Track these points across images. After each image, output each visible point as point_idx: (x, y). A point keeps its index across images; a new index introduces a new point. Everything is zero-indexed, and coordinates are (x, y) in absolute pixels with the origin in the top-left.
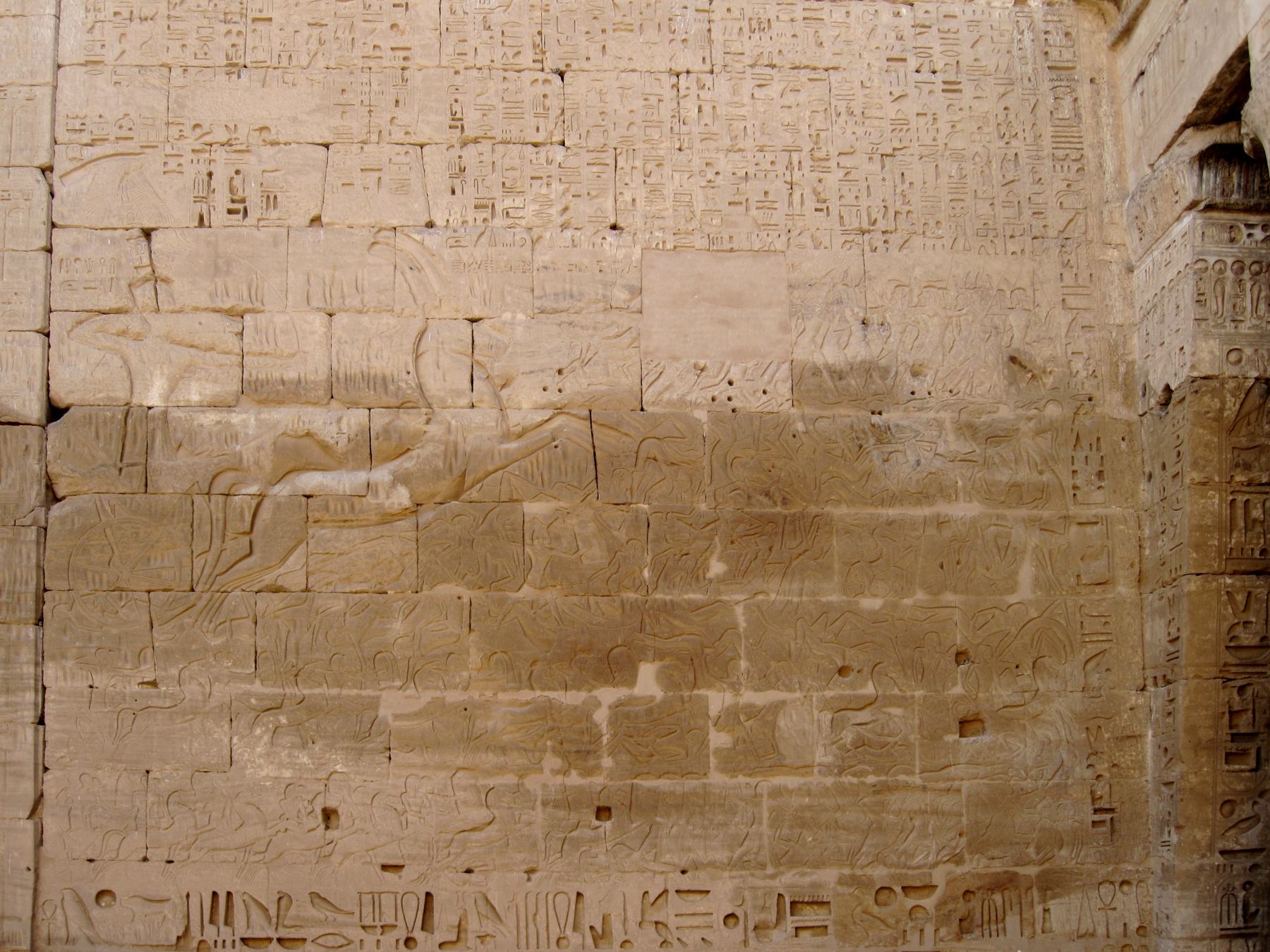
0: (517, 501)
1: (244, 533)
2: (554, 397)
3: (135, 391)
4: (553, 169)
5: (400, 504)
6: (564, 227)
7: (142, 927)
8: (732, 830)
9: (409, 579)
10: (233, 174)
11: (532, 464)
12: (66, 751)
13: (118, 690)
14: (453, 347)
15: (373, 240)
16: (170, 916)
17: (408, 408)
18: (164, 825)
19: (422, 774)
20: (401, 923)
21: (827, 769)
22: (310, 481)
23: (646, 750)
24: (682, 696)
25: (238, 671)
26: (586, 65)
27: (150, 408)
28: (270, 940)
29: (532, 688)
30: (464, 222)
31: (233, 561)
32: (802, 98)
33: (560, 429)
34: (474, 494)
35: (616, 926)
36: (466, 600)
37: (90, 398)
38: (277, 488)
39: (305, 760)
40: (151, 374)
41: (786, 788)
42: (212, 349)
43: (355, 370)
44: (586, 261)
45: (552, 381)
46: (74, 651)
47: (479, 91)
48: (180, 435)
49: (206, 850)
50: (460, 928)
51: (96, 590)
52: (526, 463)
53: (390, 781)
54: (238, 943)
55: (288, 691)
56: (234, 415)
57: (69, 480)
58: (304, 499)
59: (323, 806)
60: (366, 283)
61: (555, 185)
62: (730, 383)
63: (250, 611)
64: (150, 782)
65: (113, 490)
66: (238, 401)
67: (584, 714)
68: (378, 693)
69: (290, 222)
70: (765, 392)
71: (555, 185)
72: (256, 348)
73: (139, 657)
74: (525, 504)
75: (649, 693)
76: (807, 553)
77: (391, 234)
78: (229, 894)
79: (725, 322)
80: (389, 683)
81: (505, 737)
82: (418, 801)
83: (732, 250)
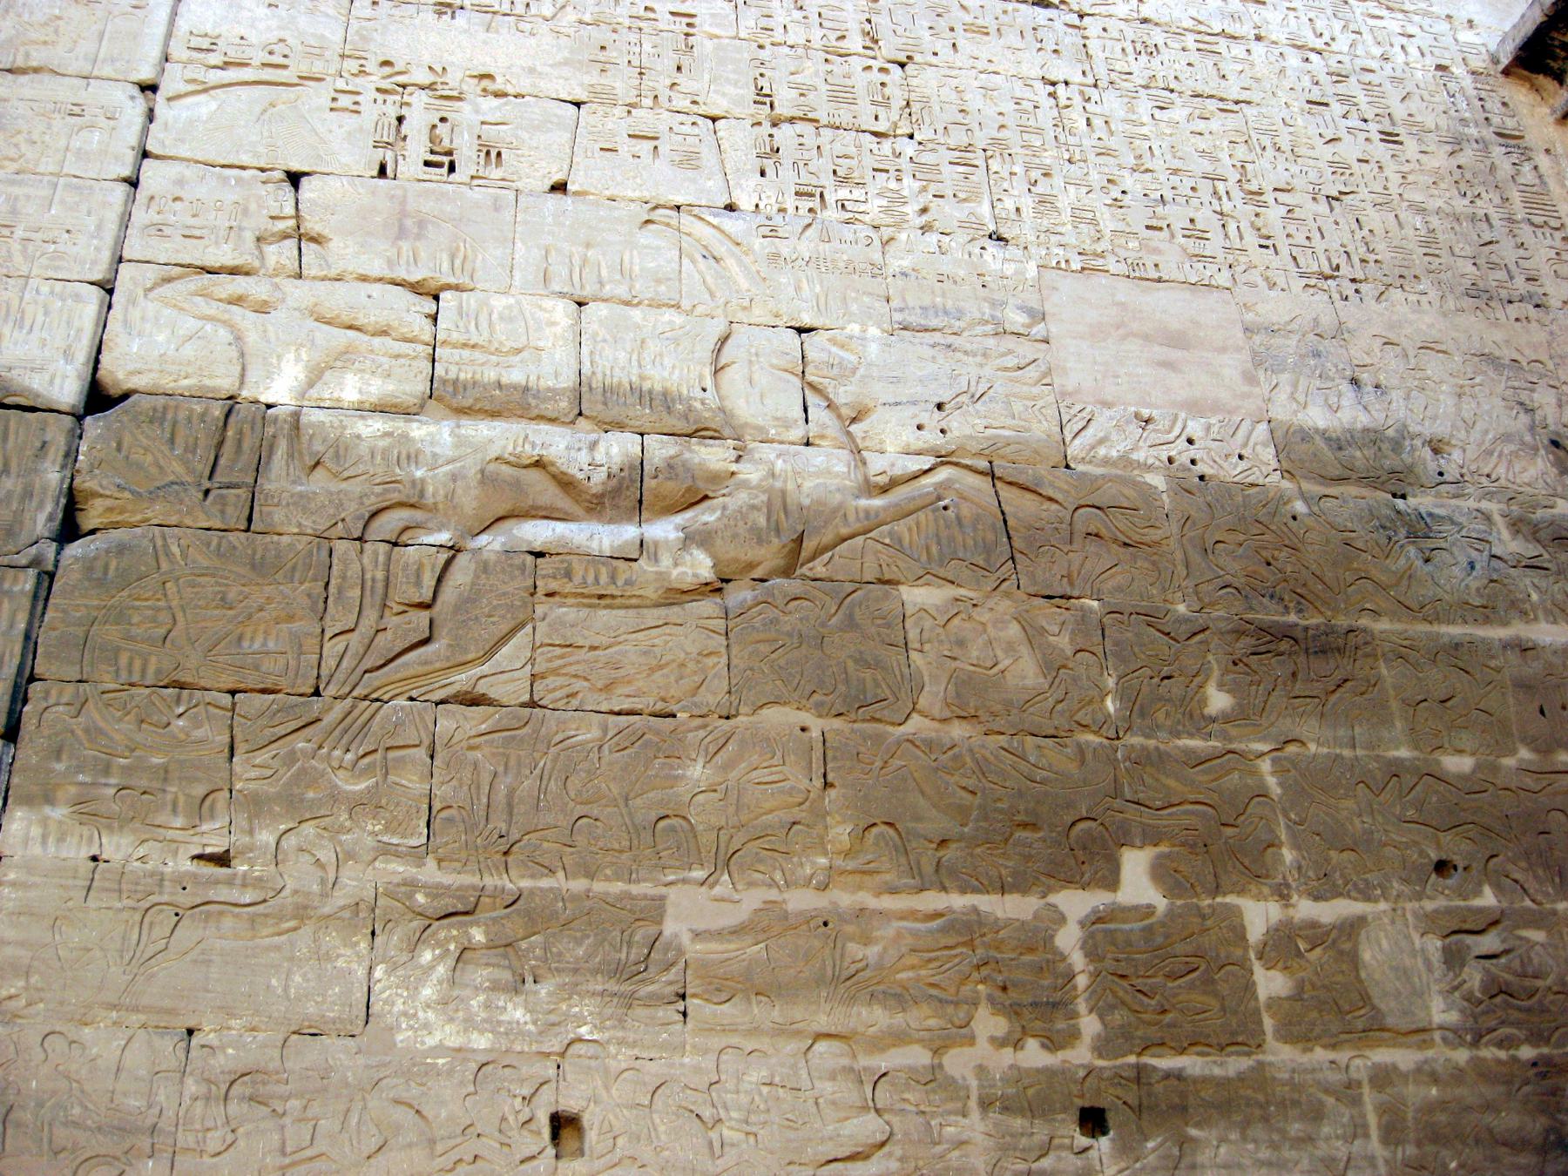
0: (888, 582)
2: (931, 438)
3: (247, 380)
4: (904, 163)
5: (695, 575)
6: (925, 229)
8: (1322, 1150)
9: (714, 696)
10: (437, 121)
11: (910, 530)
12: (21, 983)
13: (148, 867)
14: (775, 361)
15: (646, 217)
17: (704, 437)
18: (213, 1144)
19: (749, 1045)
21: (1454, 1036)
22: (538, 532)
23: (1153, 1002)
24: (1198, 908)
25: (395, 841)
26: (934, 60)
27: (269, 406)
29: (944, 889)
31: (398, 649)
32: (1214, 125)
33: (945, 485)
34: (819, 568)
36: (815, 733)
37: (167, 383)
38: (483, 539)
39: (519, 1014)
40: (279, 357)
41: (1395, 1067)
42: (384, 333)
44: (962, 273)
45: (932, 419)
46: (73, 790)
47: (793, 69)
48: (318, 447)
51: (132, 685)
52: (901, 527)
53: (686, 1060)
56: (415, 425)
57: (109, 502)
58: (530, 558)
59: (553, 1110)
60: (636, 268)
61: (907, 181)
62: (1190, 441)
63: (424, 736)
64: (193, 1054)
65: (188, 522)
66: (422, 407)
67: (1037, 938)
68: (663, 890)
69: (519, 185)
70: (1241, 457)
71: (907, 181)
72: (455, 336)
73: (201, 808)
74: (902, 588)
75: (1144, 901)
76: (1349, 684)
77: (674, 213)
79: (1167, 365)
82: (744, 1099)
83: (1159, 280)
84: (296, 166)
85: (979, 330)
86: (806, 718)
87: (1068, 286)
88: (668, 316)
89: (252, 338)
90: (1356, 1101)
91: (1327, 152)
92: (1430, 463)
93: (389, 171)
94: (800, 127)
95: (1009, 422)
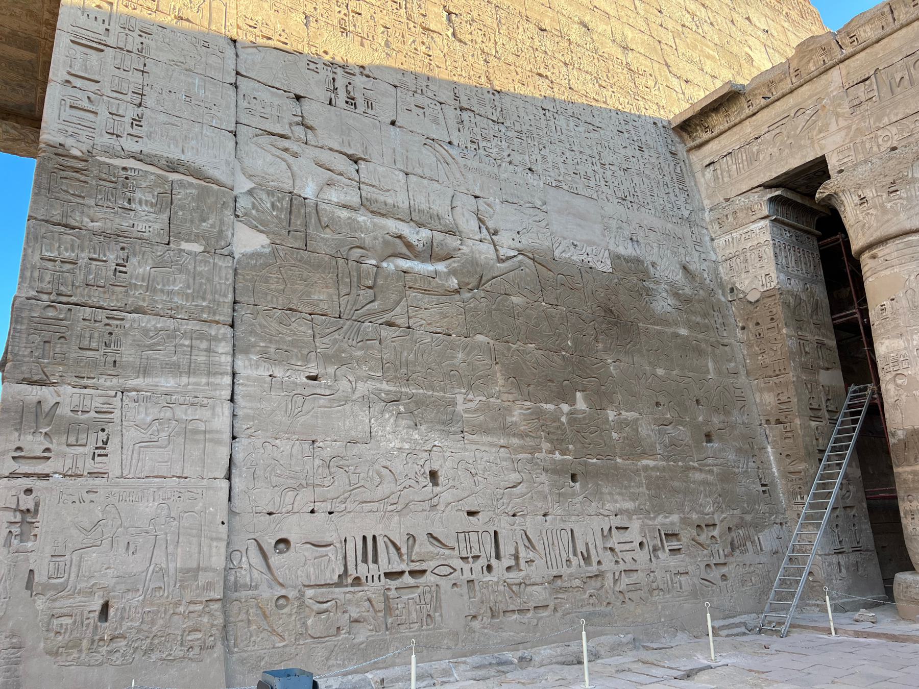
1: (370, 288)
7: (312, 569)
16: (333, 558)
20: (483, 554)
28: (402, 573)
29: (531, 401)
30: (466, 147)
33: (520, 262)
35: (593, 552)
39: (417, 436)
41: (649, 466)
42: (342, 175)
43: (424, 206)
45: (515, 236)
49: (358, 502)
50: (517, 558)
54: (382, 577)
55: (403, 390)
69: (379, 119)
72: (367, 181)
73: (306, 359)
78: (374, 537)
80: (458, 390)
81: (522, 428)
83: (577, 194)
84: (298, 93)
85: (527, 205)
86: (486, 339)
87: (552, 191)
88: (435, 184)
89: (295, 168)
90: (640, 475)
91: (623, 151)
92: (652, 270)
93: (333, 103)
94: (469, 113)
95: (538, 241)
